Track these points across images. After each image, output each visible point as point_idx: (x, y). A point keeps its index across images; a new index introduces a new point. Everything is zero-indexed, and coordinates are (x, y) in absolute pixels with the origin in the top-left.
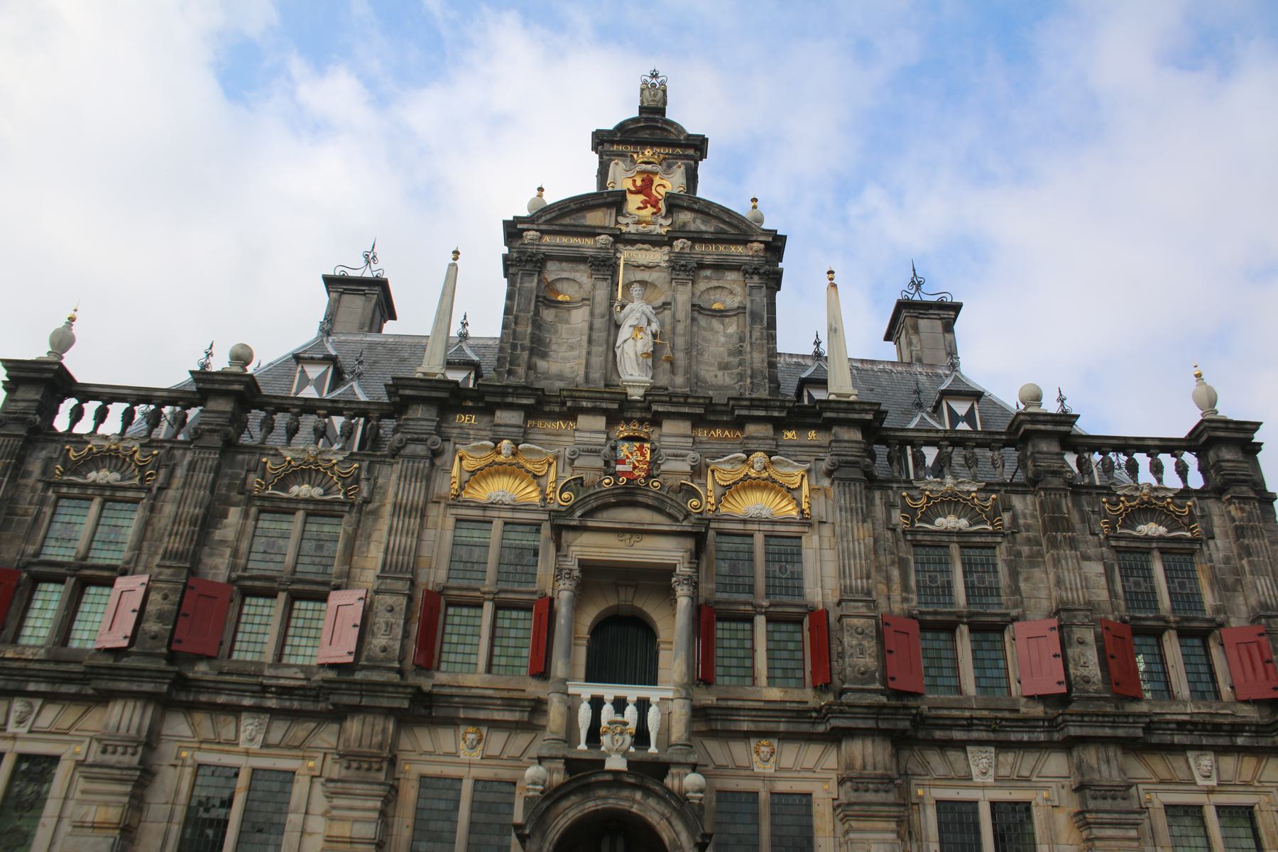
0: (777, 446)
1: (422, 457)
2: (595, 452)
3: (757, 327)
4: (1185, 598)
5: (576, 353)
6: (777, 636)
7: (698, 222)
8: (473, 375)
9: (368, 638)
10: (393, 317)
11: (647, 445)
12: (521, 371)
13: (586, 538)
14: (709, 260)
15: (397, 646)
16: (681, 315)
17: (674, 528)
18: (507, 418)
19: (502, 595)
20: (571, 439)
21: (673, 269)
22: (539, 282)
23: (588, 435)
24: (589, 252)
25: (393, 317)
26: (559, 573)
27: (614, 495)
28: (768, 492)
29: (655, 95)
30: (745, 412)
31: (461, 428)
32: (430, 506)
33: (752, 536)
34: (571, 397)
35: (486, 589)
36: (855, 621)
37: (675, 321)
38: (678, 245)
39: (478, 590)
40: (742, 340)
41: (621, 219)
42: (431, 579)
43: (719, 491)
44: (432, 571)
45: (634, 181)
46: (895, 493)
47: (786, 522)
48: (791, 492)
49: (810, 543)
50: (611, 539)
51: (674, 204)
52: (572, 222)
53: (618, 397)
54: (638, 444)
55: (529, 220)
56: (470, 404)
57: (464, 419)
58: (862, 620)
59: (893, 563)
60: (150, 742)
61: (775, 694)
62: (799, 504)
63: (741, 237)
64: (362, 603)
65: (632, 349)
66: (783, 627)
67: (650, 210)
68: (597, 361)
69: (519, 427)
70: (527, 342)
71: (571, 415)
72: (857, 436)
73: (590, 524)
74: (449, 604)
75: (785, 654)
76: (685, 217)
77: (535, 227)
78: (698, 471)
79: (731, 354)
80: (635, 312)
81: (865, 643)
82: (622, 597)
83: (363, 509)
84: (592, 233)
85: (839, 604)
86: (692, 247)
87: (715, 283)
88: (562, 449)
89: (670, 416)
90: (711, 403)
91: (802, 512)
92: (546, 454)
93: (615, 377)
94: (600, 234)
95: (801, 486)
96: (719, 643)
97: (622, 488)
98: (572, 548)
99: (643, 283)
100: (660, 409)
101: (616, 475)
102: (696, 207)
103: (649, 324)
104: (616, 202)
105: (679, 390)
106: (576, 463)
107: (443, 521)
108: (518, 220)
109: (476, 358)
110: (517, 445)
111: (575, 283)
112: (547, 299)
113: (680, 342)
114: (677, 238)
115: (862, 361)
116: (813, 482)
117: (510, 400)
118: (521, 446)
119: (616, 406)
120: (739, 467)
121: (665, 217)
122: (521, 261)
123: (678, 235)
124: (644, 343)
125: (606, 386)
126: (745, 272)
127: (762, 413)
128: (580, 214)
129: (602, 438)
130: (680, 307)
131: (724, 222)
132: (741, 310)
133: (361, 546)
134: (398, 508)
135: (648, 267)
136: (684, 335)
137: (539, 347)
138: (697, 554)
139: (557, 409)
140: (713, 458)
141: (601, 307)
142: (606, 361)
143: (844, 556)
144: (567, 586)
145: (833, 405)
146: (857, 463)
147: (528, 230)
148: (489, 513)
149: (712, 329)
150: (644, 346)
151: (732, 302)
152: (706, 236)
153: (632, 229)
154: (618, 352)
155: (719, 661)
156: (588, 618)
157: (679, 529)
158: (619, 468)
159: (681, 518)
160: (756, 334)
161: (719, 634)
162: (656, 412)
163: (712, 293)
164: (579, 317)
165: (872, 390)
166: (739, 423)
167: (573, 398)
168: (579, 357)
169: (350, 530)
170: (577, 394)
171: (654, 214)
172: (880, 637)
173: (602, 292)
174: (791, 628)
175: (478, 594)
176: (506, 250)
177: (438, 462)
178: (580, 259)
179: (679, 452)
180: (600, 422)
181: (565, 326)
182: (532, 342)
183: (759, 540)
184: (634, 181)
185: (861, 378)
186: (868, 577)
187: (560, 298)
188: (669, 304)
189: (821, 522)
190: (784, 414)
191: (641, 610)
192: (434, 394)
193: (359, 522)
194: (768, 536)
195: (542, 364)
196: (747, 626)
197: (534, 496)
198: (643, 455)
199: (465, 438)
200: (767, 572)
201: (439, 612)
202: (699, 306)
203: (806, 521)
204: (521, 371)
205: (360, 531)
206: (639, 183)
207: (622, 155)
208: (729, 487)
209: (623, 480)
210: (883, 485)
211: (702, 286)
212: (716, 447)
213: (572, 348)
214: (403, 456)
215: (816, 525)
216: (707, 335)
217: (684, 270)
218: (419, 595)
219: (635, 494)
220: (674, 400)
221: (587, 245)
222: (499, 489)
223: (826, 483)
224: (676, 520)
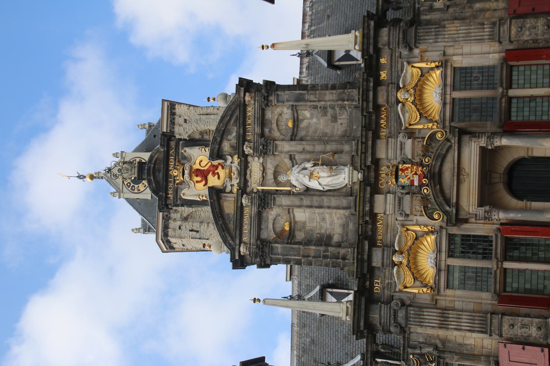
0: (392, 83)
1: (407, 312)
2: (400, 200)
3: (307, 97)
5: (327, 216)
6: (521, 82)
7: (230, 137)
8: (329, 290)
9: (531, 340)
10: (263, 359)
11: (400, 167)
12: (342, 251)
13: (464, 203)
14: (258, 130)
15: (536, 320)
16: (300, 148)
17: (456, 148)
18: (377, 259)
19: (499, 256)
20: (390, 216)
21: (265, 153)
22: (276, 243)
23: (388, 206)
24: (255, 210)
25: (263, 359)
26: (487, 218)
27: (435, 186)
28: (425, 88)
29: (127, 170)
30: (371, 105)
31: (384, 288)
32: (438, 306)
33: (454, 99)
34: (363, 217)
35: (495, 266)
36: (513, 32)
37: (304, 151)
38: (247, 150)
39: (496, 271)
40: (315, 107)
41: (228, 189)
42: (489, 302)
43: (423, 120)
44: (483, 302)
45: (197, 182)
46: (422, 6)
47: (444, 77)
48: (424, 74)
49: (459, 61)
50: (464, 188)
51: (217, 154)
52: (232, 222)
53: (362, 187)
54: (400, 172)
55: (232, 250)
56: (368, 283)
57: (377, 287)
58: (513, 28)
59: (471, 7)
62: (432, 69)
63: (242, 108)
64: (508, 345)
66: (515, 78)
67: (220, 170)
68: (334, 202)
69: (383, 250)
70: (322, 248)
71: (374, 216)
72: (385, 31)
73: (455, 200)
74: (505, 291)
75: (534, 77)
76: (226, 146)
77: (237, 247)
78: (411, 134)
79: (325, 114)
80: (297, 178)
81: (528, 26)
82: (497, 180)
84: (240, 209)
85: (500, 42)
86: (249, 141)
87: (274, 126)
88: (397, 222)
89: (374, 153)
90: (364, 127)
91: (437, 67)
92: (401, 232)
93: (344, 190)
94: (242, 203)
95: (420, 68)
96: (526, 119)
97: (430, 181)
98: (471, 211)
99: (276, 174)
100: (370, 159)
101: (421, 185)
102: (219, 139)
103: (305, 169)
104: (216, 193)
105: (354, 148)
106: (408, 212)
107: (449, 296)
108: (233, 259)
109: (318, 288)
110: (396, 251)
111: (276, 218)
112: (289, 237)
113: (319, 148)
114: (243, 151)
115: (304, 22)
116: (416, 60)
117: (366, 257)
118: (397, 249)
119: (368, 188)
120: (407, 108)
121: (226, 160)
122: (262, 256)
123: (241, 151)
125: (351, 195)
126: (267, 105)
127: (371, 94)
128: (226, 218)
129: (390, 197)
130: (293, 149)
131: (230, 120)
132: (294, 108)
133: (467, 350)
134: (443, 326)
135: (264, 171)
136: (314, 145)
137: (325, 241)
138: (473, 134)
139: (370, 226)
140: (401, 124)
141: (296, 201)
142: (333, 196)
143: (468, 38)
144: (496, 214)
145: (365, 47)
146: (404, 31)
147: (240, 252)
148: (443, 267)
149: (307, 127)
150: (324, 171)
151: (287, 113)
152: (242, 132)
153: (235, 182)
154: (327, 188)
155: (538, 118)
156: (514, 202)
157: (457, 145)
158: (416, 183)
159: (449, 144)
160: (312, 98)
161: (520, 119)
162: (372, 162)
163: (281, 128)
164: (300, 215)
165: (328, 16)
166: (377, 108)
167: (363, 217)
168: (331, 214)
169: (456, 357)
170: (361, 213)
171: (223, 168)
172: (523, 16)
173: (284, 201)
174: (515, 73)
175: (498, 271)
176: (256, 266)
177: (408, 302)
178: (259, 215)
179: (399, 146)
180: (379, 199)
181: (308, 224)
182: (321, 245)
183: (457, 95)
184: (197, 182)
185: (318, 24)
186: (483, 24)
187: (287, 228)
188: (291, 155)
189: (444, 54)
190: (372, 79)
191: (506, 168)
192: (363, 307)
193: (450, 352)
194: (454, 89)
195: (336, 238)
196: (514, 101)
197: (431, 239)
198: (407, 169)
199: (391, 286)
200: (478, 89)
201: (511, 296)
202: (292, 135)
203: (444, 64)
204: (342, 251)
205: (457, 351)
206: (199, 179)
207: (176, 191)
208: (421, 114)
209: (425, 181)
210: (417, 14)
211: (276, 134)
212: (393, 123)
213: (324, 219)
214: (406, 324)
215: (446, 57)
216: (311, 130)
217: (266, 147)
218: (501, 308)
219: (434, 173)
220: (363, 151)
221: (249, 211)
222: (427, 263)
223: (416, 51)
224: (450, 147)
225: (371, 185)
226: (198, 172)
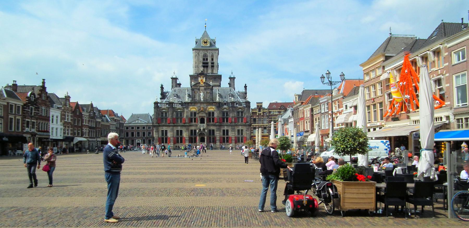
4: (242, 115)
51: (204, 83)
60: (173, 129)
65: (202, 97)
80: (202, 94)
83: (184, 111)
104: (199, 83)
217: (205, 89)
225: (201, 103)
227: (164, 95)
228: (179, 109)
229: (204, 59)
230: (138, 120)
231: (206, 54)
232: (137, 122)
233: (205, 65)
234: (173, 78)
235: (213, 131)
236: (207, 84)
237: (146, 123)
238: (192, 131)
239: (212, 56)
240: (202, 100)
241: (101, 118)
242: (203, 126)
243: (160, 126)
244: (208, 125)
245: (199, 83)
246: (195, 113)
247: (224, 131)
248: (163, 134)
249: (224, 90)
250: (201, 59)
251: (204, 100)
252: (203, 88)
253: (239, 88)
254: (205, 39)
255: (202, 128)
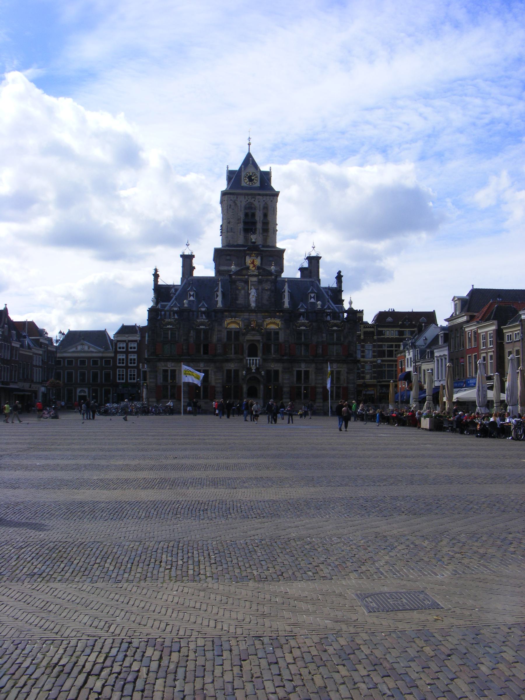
51: (258, 268)
57: (226, 314)
61: (274, 356)
65: (252, 298)
76: (261, 271)
78: (263, 321)
124: (254, 299)
180: (247, 314)
207: (248, 254)
217: (260, 282)
226: (253, 261)
227: (162, 292)
228: (202, 324)
229: (246, 215)
230: (82, 344)
231: (251, 203)
232: (79, 348)
233: (249, 226)
234: (183, 256)
235: (276, 372)
236: (264, 270)
237: (99, 352)
238: (229, 371)
239: (266, 208)
240: (253, 305)
241: (20, 341)
242: (254, 362)
243: (160, 360)
244: (265, 360)
245: (248, 268)
246: (237, 333)
247: (299, 373)
248: (165, 378)
249: (292, 281)
250: (242, 215)
251: (257, 306)
252: (255, 279)
253: (326, 279)
254: (251, 170)
255: (254, 368)
